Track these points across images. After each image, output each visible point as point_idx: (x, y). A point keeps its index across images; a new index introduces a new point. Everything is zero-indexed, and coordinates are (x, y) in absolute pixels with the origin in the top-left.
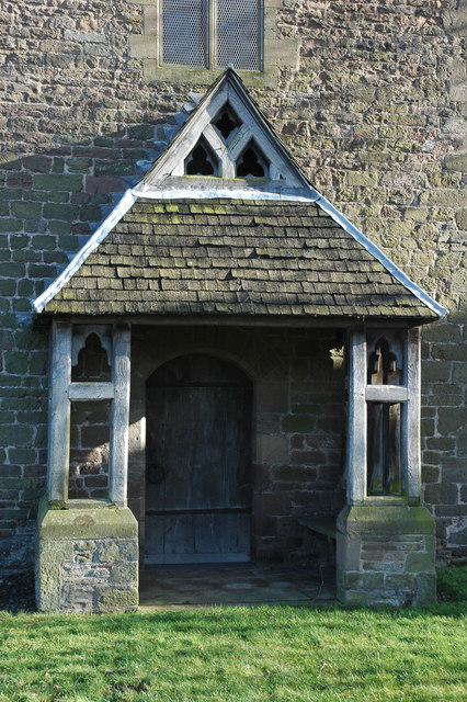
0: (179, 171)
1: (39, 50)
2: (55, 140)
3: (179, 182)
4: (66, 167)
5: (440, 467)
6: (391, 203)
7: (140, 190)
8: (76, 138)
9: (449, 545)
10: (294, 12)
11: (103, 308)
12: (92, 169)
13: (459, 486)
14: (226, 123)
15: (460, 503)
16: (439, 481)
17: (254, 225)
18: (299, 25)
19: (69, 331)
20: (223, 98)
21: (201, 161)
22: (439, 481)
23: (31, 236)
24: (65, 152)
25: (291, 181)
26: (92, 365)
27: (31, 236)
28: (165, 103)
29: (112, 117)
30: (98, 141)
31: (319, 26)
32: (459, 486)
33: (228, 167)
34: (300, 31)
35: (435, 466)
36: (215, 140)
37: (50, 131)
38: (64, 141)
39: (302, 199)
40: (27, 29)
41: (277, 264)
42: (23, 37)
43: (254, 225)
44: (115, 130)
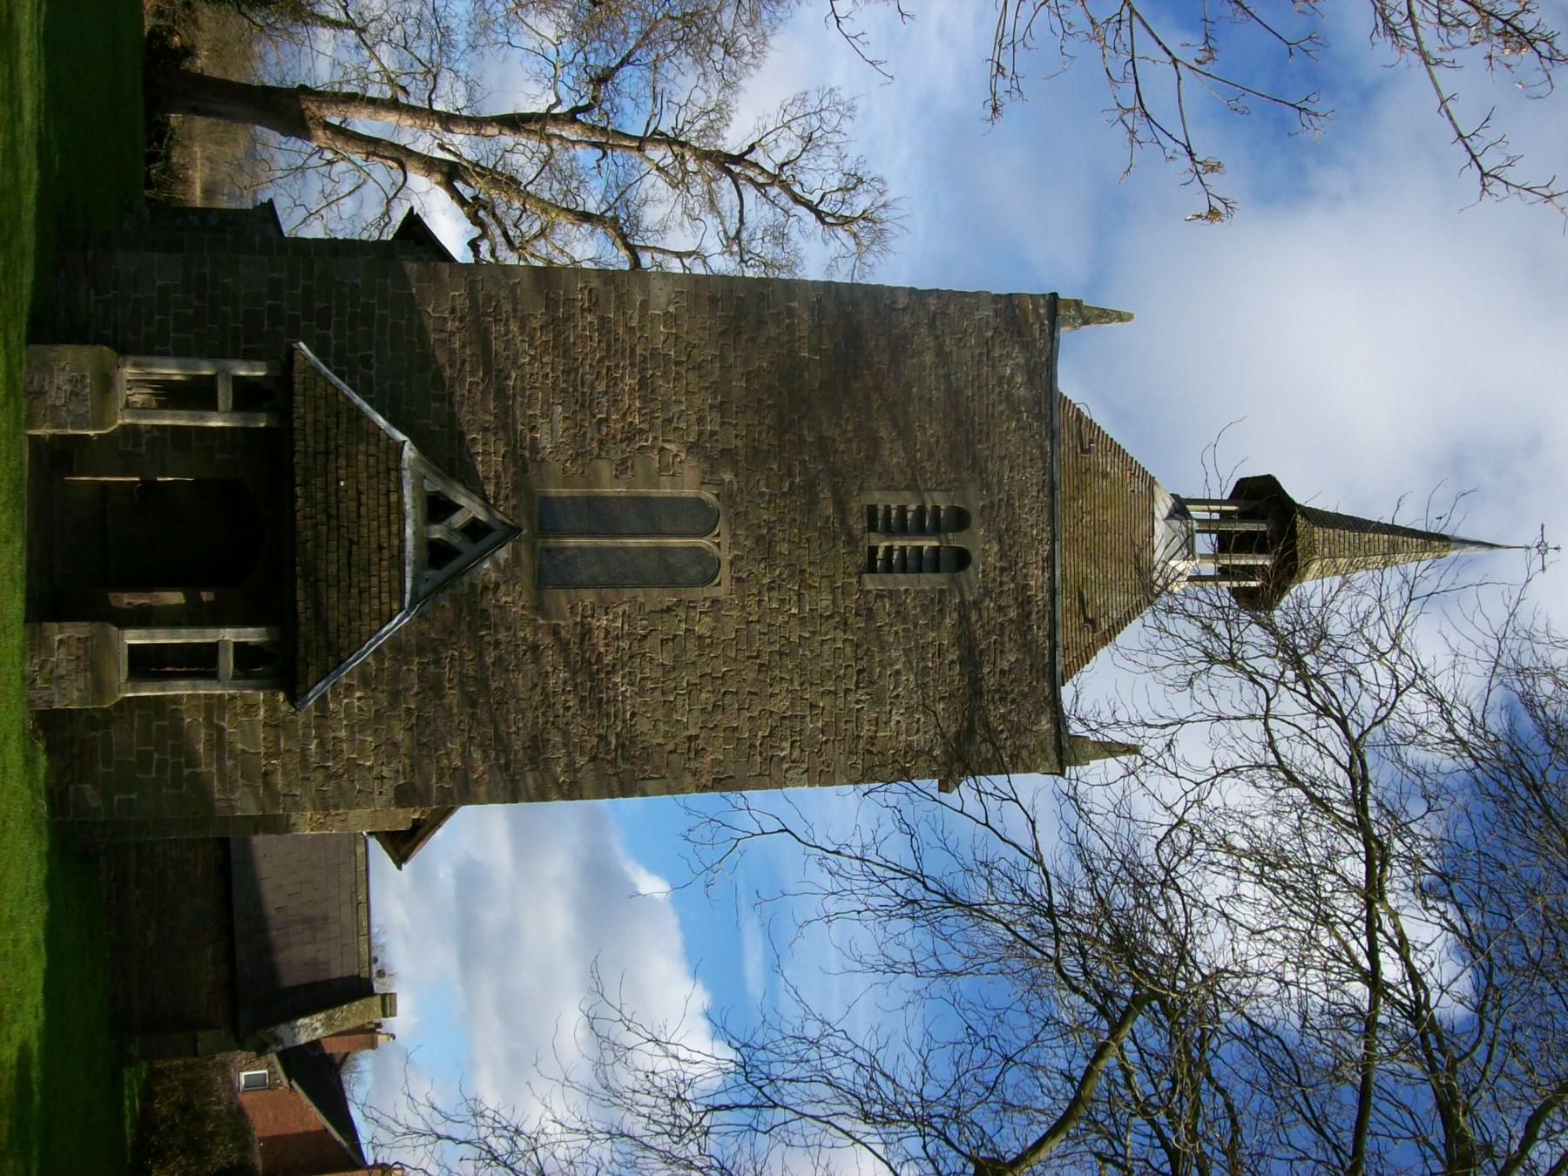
0: (429, 487)
1: (542, 383)
2: (462, 395)
3: (418, 487)
4: (437, 405)
5: (153, 775)
6: (418, 718)
7: (410, 449)
8: (464, 415)
9: (71, 788)
10: (592, 616)
11: (299, 399)
12: (437, 428)
13: (134, 796)
14: (474, 530)
15: (116, 798)
16: (139, 775)
17: (380, 548)
18: (582, 622)
19: (278, 373)
20: (498, 527)
21: (438, 508)
22: (139, 775)
23: (373, 372)
24: (451, 404)
25: (424, 588)
26: (248, 395)
27: (373, 372)
28: (501, 497)
29: (486, 448)
30: (462, 435)
31: (582, 641)
32: (134, 796)
33: (437, 532)
34: (576, 623)
35: (154, 770)
36: (458, 520)
37: (469, 391)
38: (462, 404)
39: (408, 597)
40: (559, 373)
41: (344, 560)
42: (552, 370)
43: (380, 548)
44: (472, 451)
